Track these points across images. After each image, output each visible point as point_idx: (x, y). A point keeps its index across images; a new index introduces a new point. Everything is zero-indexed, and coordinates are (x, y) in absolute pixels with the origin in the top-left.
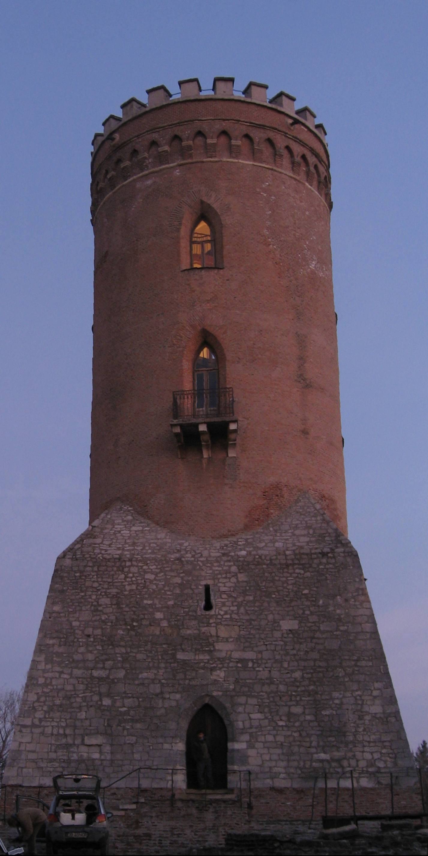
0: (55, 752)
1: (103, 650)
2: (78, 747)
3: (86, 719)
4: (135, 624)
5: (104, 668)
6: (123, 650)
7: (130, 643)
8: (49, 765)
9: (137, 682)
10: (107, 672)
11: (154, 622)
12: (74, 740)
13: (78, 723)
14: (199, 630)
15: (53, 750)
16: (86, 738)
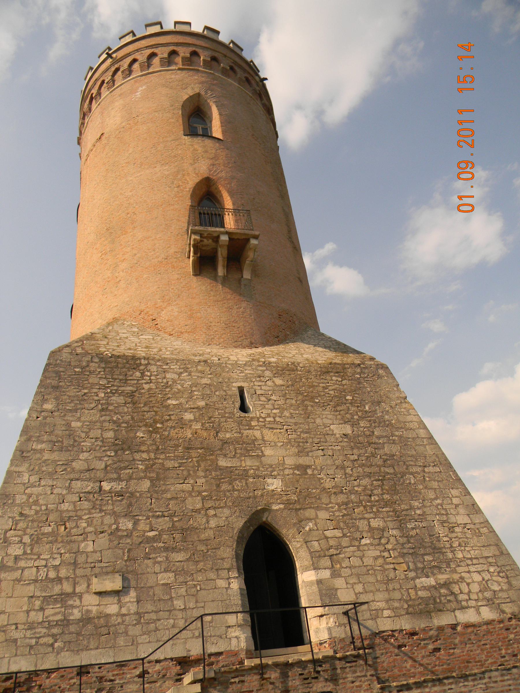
0: (42, 609)
1: (116, 455)
2: (80, 598)
3: (95, 552)
4: (158, 425)
5: (119, 479)
6: (145, 456)
7: (154, 447)
8: (29, 634)
9: (169, 496)
10: (124, 484)
11: (182, 424)
12: (75, 585)
13: (81, 559)
14: (240, 433)
15: (37, 608)
16: (95, 580)
